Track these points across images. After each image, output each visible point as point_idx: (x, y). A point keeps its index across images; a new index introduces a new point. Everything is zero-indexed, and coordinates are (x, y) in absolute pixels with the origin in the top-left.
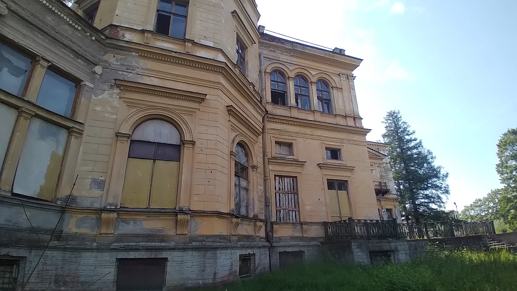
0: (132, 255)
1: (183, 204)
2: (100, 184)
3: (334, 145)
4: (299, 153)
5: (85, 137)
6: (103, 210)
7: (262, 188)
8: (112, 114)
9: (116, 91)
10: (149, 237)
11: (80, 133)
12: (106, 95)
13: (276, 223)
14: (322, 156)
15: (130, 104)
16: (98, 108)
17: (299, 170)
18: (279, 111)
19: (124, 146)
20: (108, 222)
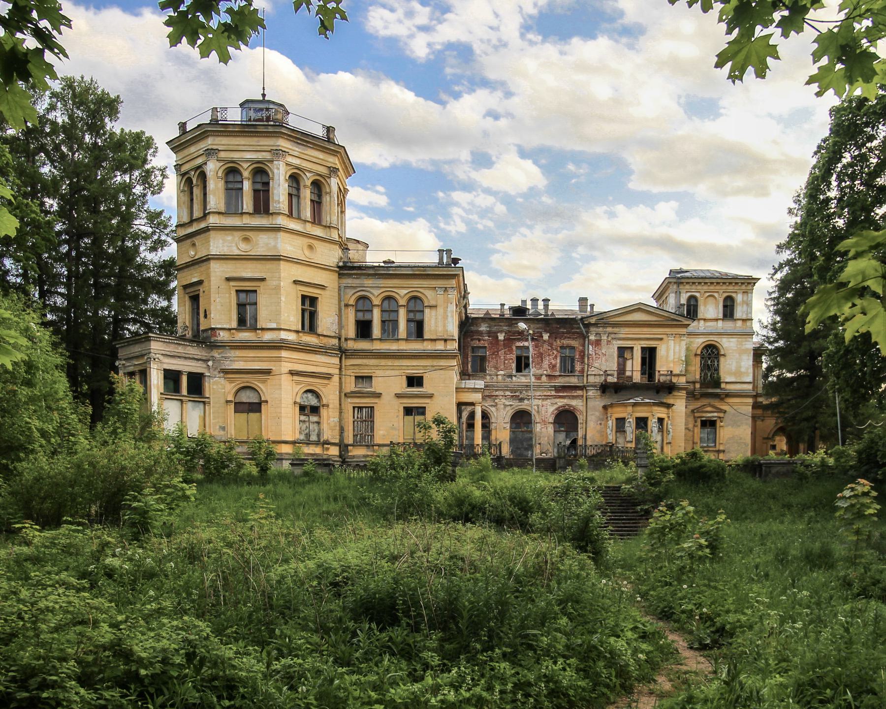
4: (377, 385)
7: (337, 419)
11: (209, 403)
13: (350, 445)
14: (401, 385)
18: (363, 345)
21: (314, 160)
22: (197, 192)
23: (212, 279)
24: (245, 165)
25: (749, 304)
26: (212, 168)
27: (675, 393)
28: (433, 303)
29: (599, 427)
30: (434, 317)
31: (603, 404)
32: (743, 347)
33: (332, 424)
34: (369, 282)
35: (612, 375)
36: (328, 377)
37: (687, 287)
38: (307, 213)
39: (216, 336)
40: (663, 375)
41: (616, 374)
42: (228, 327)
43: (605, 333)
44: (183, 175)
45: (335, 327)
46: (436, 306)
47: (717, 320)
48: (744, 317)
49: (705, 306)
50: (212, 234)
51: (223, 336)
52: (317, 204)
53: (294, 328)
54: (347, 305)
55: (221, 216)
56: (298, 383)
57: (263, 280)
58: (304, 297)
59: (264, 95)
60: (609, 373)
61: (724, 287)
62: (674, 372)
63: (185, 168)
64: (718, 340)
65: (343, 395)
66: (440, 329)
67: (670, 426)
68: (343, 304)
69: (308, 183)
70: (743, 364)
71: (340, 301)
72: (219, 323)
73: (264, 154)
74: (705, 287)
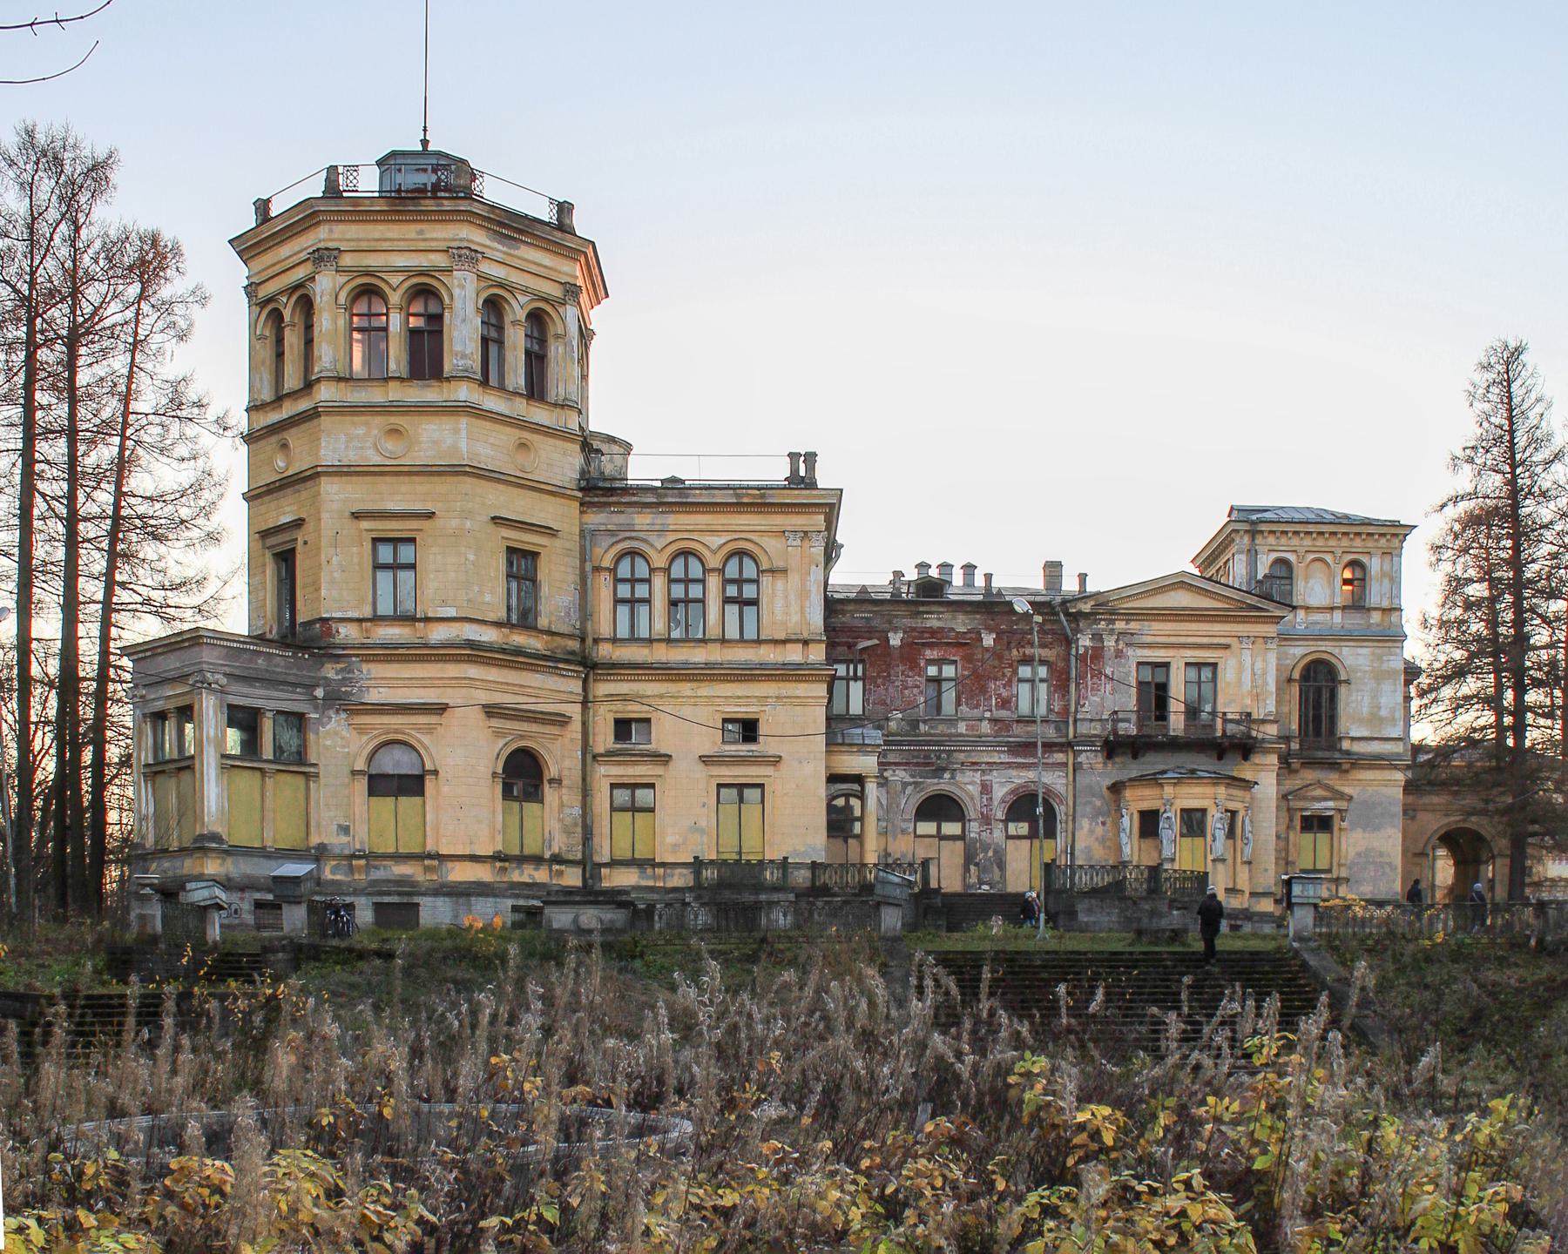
0: (387, 899)
1: (430, 847)
2: (345, 830)
3: (743, 711)
5: (322, 780)
6: (353, 856)
7: (577, 811)
8: (344, 747)
9: (343, 715)
10: (402, 882)
11: (317, 775)
12: (332, 726)
13: (605, 865)
14: (710, 742)
15: (361, 730)
16: (328, 743)
17: (659, 770)
19: (362, 785)
20: (359, 868)
21: (533, 269)
22: (292, 339)
23: (325, 516)
24: (395, 280)
25: (1394, 579)
26: (326, 286)
27: (1257, 759)
28: (778, 563)
29: (1099, 830)
30: (779, 594)
31: (1109, 782)
32: (1385, 667)
33: (568, 821)
34: (642, 520)
35: (1128, 721)
36: (562, 721)
37: (1271, 540)
38: (517, 376)
39: (330, 635)
40: (1231, 721)
41: (1134, 717)
42: (356, 615)
43: (1112, 632)
44: (263, 304)
45: (575, 615)
46: (784, 571)
47: (1332, 609)
48: (1385, 604)
49: (1307, 578)
50: (325, 421)
51: (347, 633)
52: (536, 361)
53: (491, 617)
54: (597, 569)
55: (342, 385)
56: (499, 734)
57: (430, 515)
58: (511, 551)
59: (425, 142)
60: (1121, 715)
61: (1345, 542)
62: (1255, 716)
63: (265, 291)
64: (1336, 651)
65: (589, 758)
66: (795, 618)
67: (1248, 828)
68: (588, 567)
69: (521, 315)
70: (1383, 700)
71: (583, 560)
72: (340, 609)
73: (432, 256)
74: (1308, 542)
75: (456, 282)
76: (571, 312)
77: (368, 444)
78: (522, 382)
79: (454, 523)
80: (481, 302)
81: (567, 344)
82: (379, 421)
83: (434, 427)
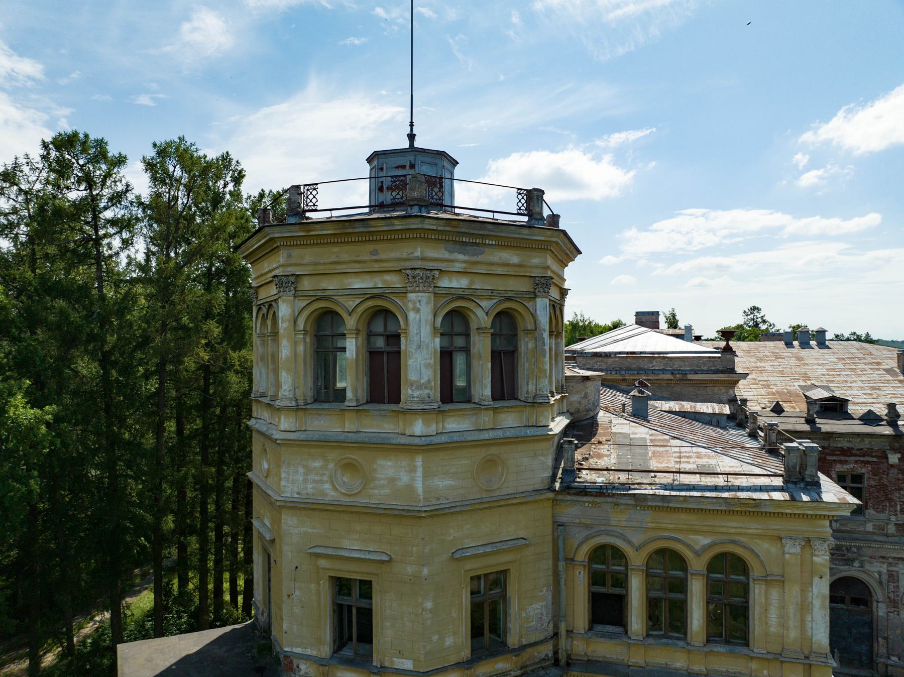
21: (500, 270)
24: (351, 304)
73: (388, 277)
75: (410, 305)
76: (542, 306)
77: (325, 478)
78: (488, 392)
79: (410, 570)
80: (439, 320)
81: (539, 340)
82: (333, 455)
83: (389, 463)
